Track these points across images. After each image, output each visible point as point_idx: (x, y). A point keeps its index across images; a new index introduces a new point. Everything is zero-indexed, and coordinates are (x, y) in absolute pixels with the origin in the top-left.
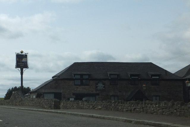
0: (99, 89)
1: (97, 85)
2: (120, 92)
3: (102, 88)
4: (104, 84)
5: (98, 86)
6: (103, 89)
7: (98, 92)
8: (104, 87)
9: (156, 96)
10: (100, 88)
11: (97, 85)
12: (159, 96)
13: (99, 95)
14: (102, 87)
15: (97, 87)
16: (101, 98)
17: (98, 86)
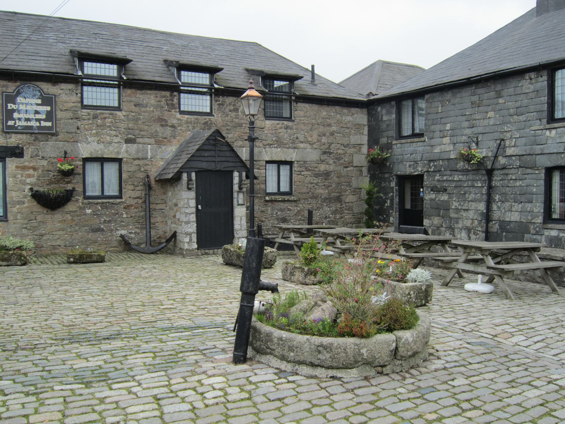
0: (18, 123)
1: (10, 106)
2: (128, 141)
3: (38, 120)
4: (47, 100)
5: (14, 106)
6: (43, 124)
7: (13, 140)
8: (50, 116)
9: (279, 163)
10: (28, 120)
11: (10, 106)
12: (290, 163)
13: (22, 157)
14: (38, 116)
15: (9, 114)
16: (31, 172)
17: (14, 106)
